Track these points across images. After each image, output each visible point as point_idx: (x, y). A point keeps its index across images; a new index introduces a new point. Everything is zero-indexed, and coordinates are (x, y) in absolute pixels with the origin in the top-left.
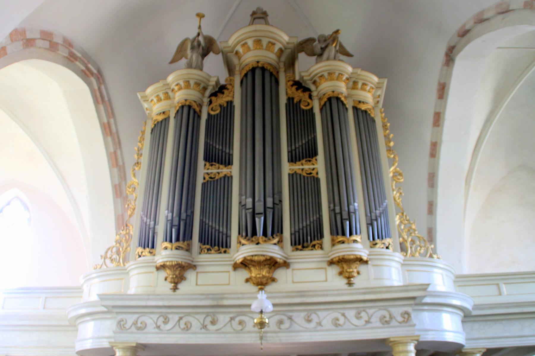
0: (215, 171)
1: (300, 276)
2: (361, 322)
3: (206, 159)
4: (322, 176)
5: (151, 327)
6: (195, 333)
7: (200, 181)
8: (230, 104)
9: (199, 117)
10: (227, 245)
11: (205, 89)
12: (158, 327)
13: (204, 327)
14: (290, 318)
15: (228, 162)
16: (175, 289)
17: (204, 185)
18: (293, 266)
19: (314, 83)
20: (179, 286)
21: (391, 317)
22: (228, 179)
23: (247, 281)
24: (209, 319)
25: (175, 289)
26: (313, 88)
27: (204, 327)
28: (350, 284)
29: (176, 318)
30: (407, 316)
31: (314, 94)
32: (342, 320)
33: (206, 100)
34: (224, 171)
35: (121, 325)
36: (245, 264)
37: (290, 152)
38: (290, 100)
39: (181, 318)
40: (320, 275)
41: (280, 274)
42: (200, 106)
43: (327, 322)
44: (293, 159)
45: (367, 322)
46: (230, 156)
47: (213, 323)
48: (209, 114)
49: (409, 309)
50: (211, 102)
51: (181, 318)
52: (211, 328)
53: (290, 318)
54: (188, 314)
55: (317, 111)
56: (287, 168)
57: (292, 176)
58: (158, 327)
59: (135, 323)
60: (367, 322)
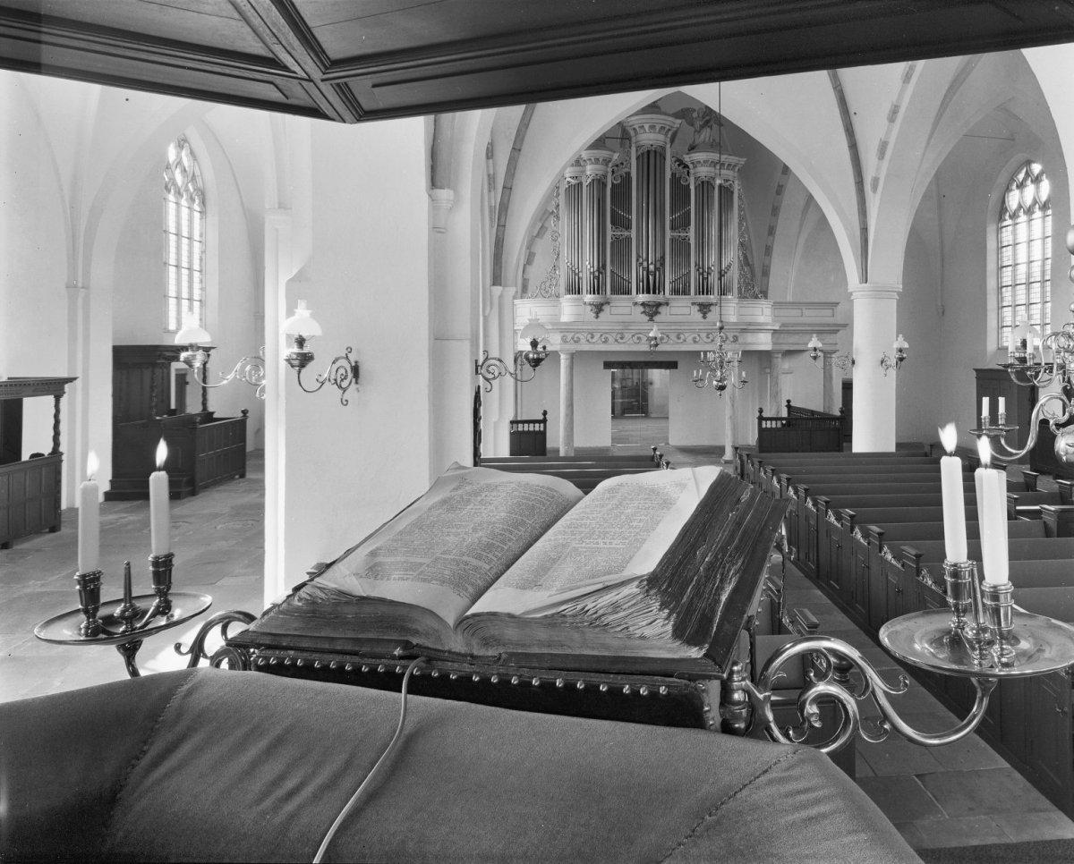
0: (619, 233)
1: (674, 311)
2: (710, 340)
3: (613, 223)
4: (692, 242)
5: (583, 341)
6: (611, 344)
7: (609, 241)
8: (628, 174)
9: (606, 186)
10: (629, 292)
11: (610, 161)
12: (588, 341)
13: (616, 340)
14: (668, 336)
15: (628, 227)
16: (597, 317)
17: (612, 244)
18: (671, 305)
19: (693, 163)
20: (601, 315)
21: (727, 338)
22: (629, 239)
23: (644, 312)
24: (619, 336)
25: (597, 317)
26: (691, 166)
27: (616, 340)
28: (704, 317)
29: (599, 335)
30: (736, 339)
31: (692, 171)
32: (698, 338)
33: (610, 170)
34: (626, 233)
35: (564, 340)
36: (643, 304)
37: (672, 221)
38: (673, 175)
39: (601, 336)
40: (686, 311)
41: (661, 309)
42: (605, 176)
43: (690, 339)
44: (672, 228)
45: (712, 341)
46: (630, 221)
47: (622, 338)
48: (613, 183)
49: (738, 334)
50: (613, 172)
51: (601, 336)
52: (620, 340)
53: (668, 336)
54: (606, 333)
55: (692, 187)
56: (669, 234)
57: (673, 240)
58: (588, 341)
59: (572, 338)
60: (712, 341)
